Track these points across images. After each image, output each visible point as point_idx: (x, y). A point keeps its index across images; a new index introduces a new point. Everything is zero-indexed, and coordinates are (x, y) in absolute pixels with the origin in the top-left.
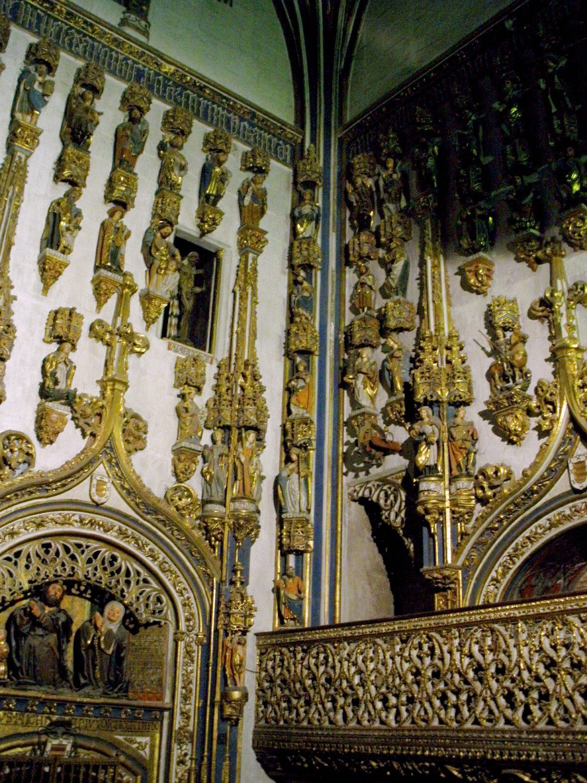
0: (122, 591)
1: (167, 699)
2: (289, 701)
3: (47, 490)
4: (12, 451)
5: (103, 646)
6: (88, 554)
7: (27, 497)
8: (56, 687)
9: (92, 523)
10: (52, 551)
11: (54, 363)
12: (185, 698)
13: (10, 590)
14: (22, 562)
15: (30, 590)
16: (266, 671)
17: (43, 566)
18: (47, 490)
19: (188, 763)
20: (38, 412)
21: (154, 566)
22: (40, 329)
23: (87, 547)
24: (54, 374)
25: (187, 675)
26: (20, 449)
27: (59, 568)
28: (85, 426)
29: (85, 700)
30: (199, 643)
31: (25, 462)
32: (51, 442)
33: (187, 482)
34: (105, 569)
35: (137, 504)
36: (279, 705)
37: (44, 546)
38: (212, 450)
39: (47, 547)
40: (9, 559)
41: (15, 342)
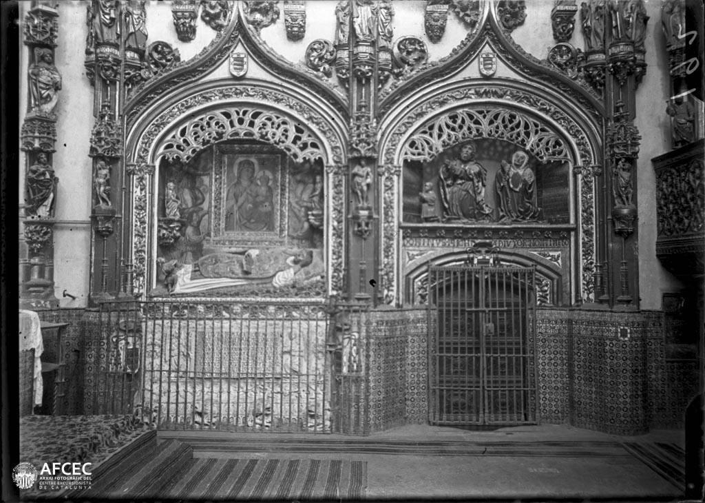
0: (523, 140)
1: (572, 221)
2: (677, 214)
5: (511, 186)
6: (489, 116)
8: (477, 220)
9: (486, 93)
10: (459, 121)
12: (587, 220)
13: (429, 154)
14: (436, 131)
16: (662, 190)
19: (595, 270)
21: (548, 118)
23: (488, 112)
25: (586, 202)
27: (467, 132)
28: (466, 18)
29: (499, 226)
30: (595, 174)
33: (571, 41)
34: (505, 127)
35: (521, 70)
36: (671, 218)
38: (589, 6)
39: (454, 118)
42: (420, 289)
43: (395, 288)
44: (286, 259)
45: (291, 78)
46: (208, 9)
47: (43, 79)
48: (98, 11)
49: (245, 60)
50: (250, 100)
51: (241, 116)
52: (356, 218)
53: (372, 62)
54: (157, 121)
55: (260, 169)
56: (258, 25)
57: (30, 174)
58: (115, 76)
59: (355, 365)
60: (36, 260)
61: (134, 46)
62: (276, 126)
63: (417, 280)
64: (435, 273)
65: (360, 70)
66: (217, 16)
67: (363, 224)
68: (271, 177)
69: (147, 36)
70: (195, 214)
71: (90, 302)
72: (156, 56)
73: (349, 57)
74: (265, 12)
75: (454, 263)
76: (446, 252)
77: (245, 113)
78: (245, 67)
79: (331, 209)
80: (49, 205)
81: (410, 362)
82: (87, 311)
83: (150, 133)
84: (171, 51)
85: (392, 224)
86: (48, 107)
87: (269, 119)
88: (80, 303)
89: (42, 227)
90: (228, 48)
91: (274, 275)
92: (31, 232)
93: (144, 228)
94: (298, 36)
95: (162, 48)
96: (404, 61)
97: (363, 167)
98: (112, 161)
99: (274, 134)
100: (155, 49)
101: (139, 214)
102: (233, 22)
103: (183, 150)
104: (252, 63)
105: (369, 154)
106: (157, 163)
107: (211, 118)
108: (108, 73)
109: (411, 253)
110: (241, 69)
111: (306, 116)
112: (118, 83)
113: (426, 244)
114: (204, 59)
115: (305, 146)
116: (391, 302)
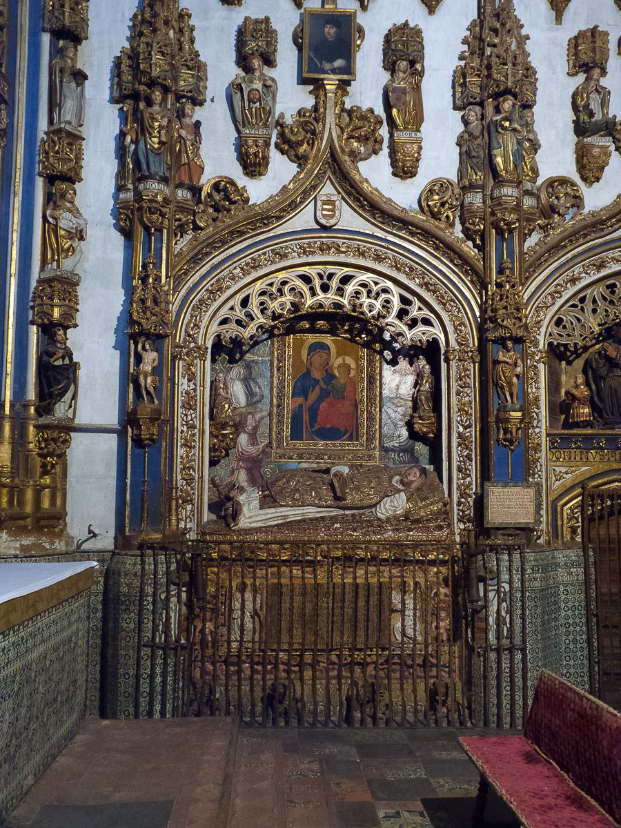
3: (602, 229)
4: (557, 198)
7: (582, 241)
11: (585, 95)
13: (581, 335)
14: (589, 306)
15: (600, 334)
17: (612, 307)
18: (602, 229)
20: (576, 152)
22: (562, 62)
24: (587, 106)
26: (566, 194)
31: (573, 206)
32: (598, 179)
37: (608, 287)
40: (574, 306)
41: (538, 84)
42: (570, 519)
43: (544, 519)
44: (391, 478)
45: (400, 229)
46: (288, 135)
47: (63, 224)
48: (143, 133)
49: (337, 203)
50: (342, 258)
51: (325, 280)
52: (507, 420)
53: (517, 208)
54: (212, 285)
55: (339, 354)
56: (355, 156)
57: (45, 358)
58: (162, 223)
59: (505, 629)
60: (47, 480)
61: (187, 181)
62: (373, 294)
63: (565, 508)
64: (590, 496)
65: (504, 220)
66: (300, 144)
67: (514, 430)
68: (353, 365)
69: (203, 169)
70: (250, 416)
71: (122, 540)
72: (217, 197)
73: (484, 202)
74: (364, 139)
75: (617, 484)
76: (606, 468)
77: (330, 276)
78: (337, 213)
79: (455, 408)
80: (69, 402)
81: (563, 621)
82: (119, 554)
83: (201, 302)
84: (237, 190)
85: (537, 430)
86: (67, 264)
87: (364, 285)
88: (107, 541)
89: (60, 433)
90: (314, 187)
91: (379, 502)
92: (46, 440)
93: (194, 435)
94: (411, 173)
95: (223, 187)
96: (553, 210)
97: (508, 351)
98: (157, 339)
99: (371, 307)
100: (216, 187)
101: (186, 415)
102: (324, 152)
103: (244, 327)
104: (345, 207)
105: (520, 333)
106: (209, 344)
107: (284, 283)
108: (155, 217)
109: (556, 468)
110: (332, 217)
111: (417, 280)
112: (165, 231)
113: (578, 459)
114: (285, 200)
115: (413, 324)
116: (539, 538)
